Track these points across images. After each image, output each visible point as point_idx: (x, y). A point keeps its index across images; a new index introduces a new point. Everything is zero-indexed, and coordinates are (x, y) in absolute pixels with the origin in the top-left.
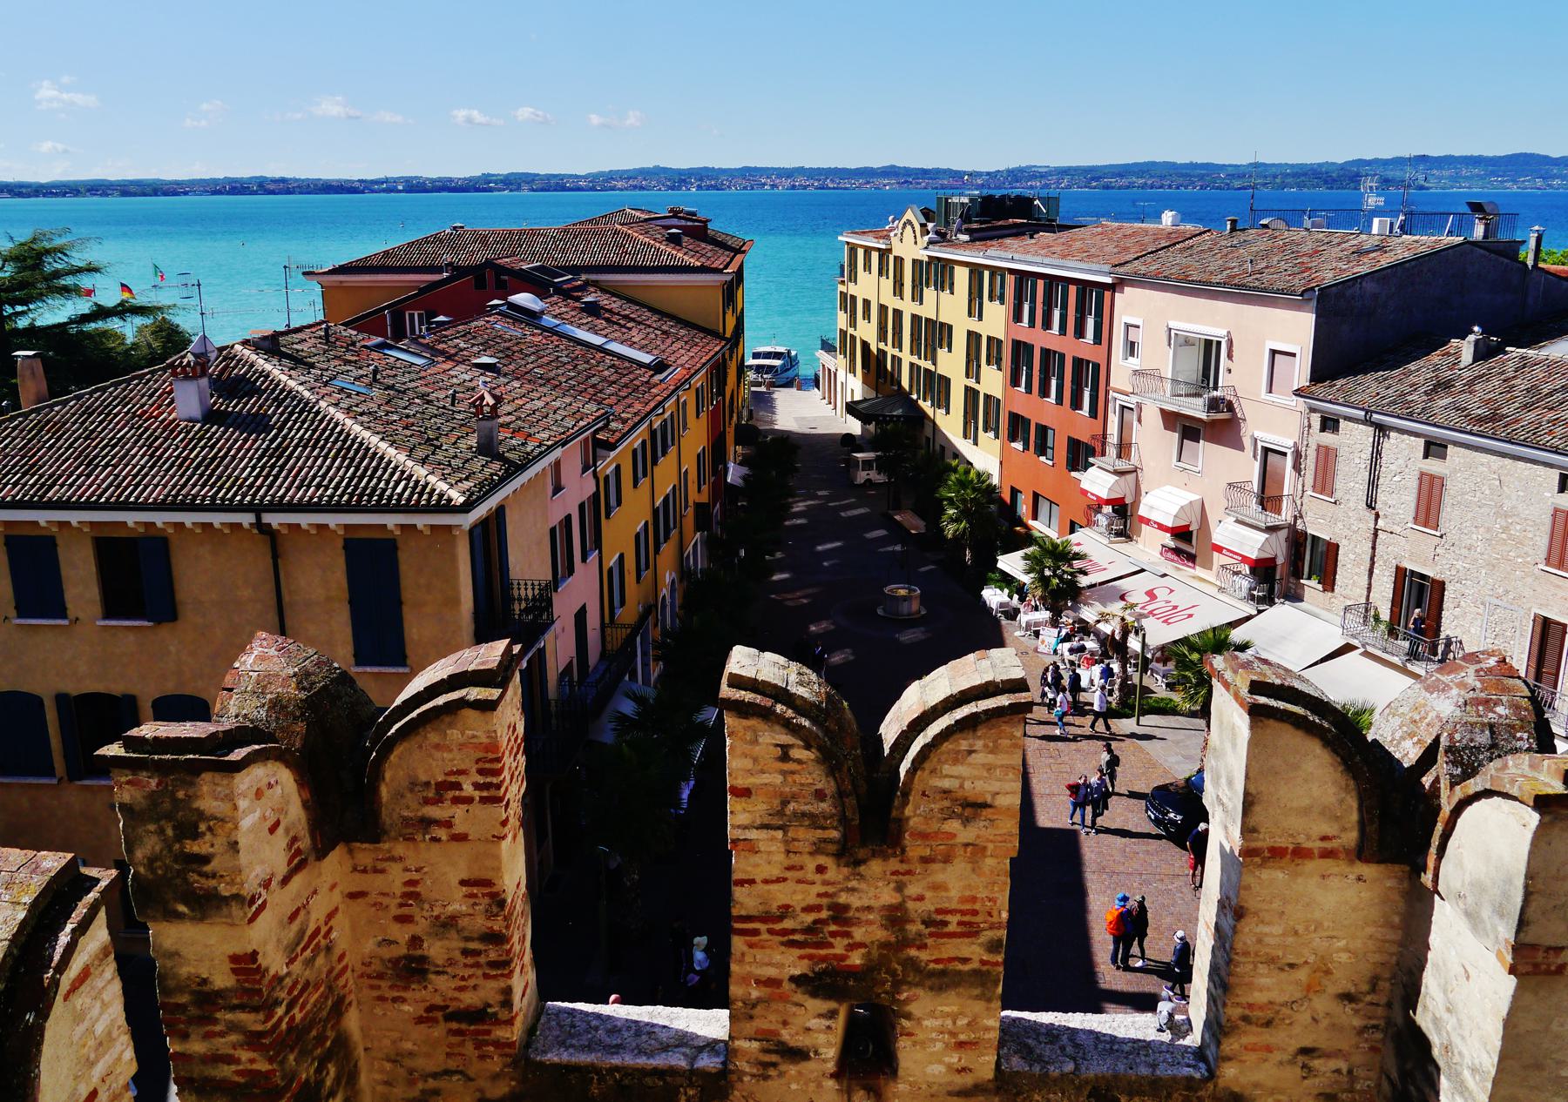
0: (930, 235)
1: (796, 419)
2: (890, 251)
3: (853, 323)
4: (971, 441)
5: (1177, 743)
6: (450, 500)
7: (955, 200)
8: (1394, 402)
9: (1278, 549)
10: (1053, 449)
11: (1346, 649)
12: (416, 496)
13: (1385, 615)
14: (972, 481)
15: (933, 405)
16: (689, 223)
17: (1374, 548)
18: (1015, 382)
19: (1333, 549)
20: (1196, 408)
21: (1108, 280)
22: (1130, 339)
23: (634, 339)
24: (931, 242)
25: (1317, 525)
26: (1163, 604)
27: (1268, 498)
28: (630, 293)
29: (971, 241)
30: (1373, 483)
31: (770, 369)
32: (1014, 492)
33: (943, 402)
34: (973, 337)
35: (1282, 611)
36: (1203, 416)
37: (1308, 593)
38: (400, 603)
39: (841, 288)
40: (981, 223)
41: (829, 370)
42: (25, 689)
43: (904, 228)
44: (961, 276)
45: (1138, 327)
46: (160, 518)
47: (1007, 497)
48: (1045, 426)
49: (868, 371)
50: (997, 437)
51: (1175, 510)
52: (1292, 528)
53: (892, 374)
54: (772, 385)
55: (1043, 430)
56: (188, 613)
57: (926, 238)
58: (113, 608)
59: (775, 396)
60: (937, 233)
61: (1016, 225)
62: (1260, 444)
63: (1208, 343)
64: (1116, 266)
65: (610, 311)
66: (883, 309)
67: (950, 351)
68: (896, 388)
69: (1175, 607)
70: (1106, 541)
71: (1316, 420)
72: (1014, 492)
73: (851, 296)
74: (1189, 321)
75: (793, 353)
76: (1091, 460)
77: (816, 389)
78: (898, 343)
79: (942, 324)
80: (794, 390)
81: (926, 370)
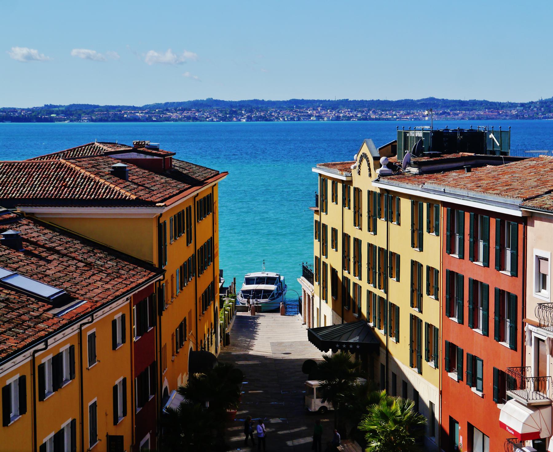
0: (382, 168)
1: (273, 344)
2: (350, 182)
3: (324, 252)
7: (411, 134)
10: (482, 379)
14: (394, 413)
15: (386, 333)
16: (148, 157)
18: (449, 312)
21: (518, 214)
22: (542, 271)
23: (48, 272)
24: (383, 175)
28: (67, 226)
29: (421, 173)
31: (266, 293)
32: (453, 422)
33: (394, 332)
34: (416, 266)
39: (316, 217)
40: (431, 156)
41: (309, 296)
43: (361, 161)
44: (406, 206)
45: (547, 260)
47: (447, 428)
48: (475, 356)
49: (337, 298)
50: (437, 366)
53: (354, 303)
54: (258, 309)
55: (473, 360)
57: (378, 171)
59: (259, 321)
60: (390, 165)
61: (463, 159)
64: (527, 199)
65: (36, 244)
66: (346, 237)
67: (398, 280)
68: (356, 315)
72: (453, 422)
73: (323, 224)
75: (282, 278)
76: (509, 393)
77: (299, 314)
78: (358, 273)
79: (392, 254)
80: (278, 315)
81: (381, 298)
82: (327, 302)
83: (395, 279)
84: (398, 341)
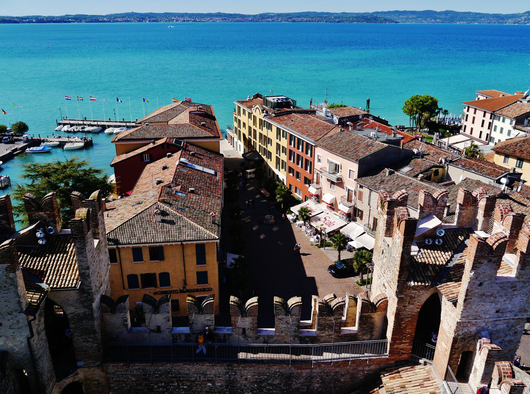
2: (252, 113)
4: (278, 170)
5: (332, 253)
9: (352, 211)
13: (372, 227)
15: (266, 157)
19: (362, 212)
20: (334, 178)
25: (359, 207)
30: (369, 200)
32: (290, 185)
35: (352, 224)
36: (336, 182)
37: (358, 220)
38: (205, 254)
44: (274, 129)
46: (163, 244)
50: (285, 171)
52: (354, 207)
53: (254, 147)
55: (298, 173)
56: (166, 259)
57: (263, 114)
58: (152, 258)
63: (336, 165)
67: (271, 145)
72: (290, 185)
79: (269, 138)
81: (264, 148)
84: (271, 161)
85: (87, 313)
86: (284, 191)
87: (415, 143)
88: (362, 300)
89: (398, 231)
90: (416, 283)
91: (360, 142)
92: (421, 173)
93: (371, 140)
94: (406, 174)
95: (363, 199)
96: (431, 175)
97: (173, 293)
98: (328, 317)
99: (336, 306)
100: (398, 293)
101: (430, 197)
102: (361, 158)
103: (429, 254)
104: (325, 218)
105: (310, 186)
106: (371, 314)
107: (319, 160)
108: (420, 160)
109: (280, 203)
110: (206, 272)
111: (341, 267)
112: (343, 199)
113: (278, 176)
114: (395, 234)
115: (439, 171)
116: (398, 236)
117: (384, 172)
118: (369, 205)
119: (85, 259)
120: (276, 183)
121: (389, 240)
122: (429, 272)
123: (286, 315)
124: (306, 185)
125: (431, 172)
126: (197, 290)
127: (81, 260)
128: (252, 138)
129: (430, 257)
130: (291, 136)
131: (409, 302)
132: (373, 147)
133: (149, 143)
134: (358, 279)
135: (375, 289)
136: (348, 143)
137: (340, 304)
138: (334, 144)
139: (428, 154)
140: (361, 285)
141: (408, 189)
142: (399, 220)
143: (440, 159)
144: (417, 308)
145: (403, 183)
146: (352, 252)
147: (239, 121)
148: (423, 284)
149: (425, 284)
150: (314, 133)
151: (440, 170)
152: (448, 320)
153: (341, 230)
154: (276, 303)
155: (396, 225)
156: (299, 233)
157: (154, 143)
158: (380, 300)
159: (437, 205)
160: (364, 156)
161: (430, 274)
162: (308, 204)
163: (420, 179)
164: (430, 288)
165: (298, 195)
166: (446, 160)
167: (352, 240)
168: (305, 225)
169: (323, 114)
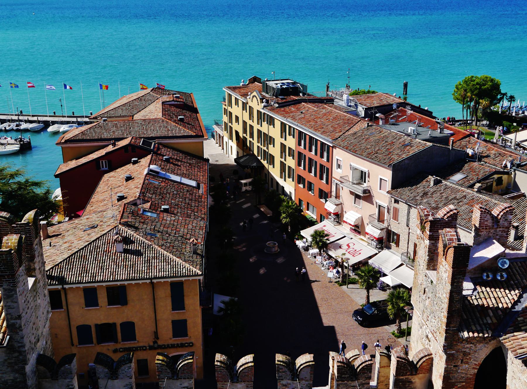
2: (247, 103)
4: (283, 179)
5: (358, 293)
6: (198, 273)
8: (412, 200)
9: (384, 235)
11: (402, 265)
12: (189, 273)
15: (267, 163)
16: (178, 103)
17: (409, 237)
19: (398, 236)
26: (352, 249)
27: (380, 219)
28: (175, 146)
30: (408, 220)
32: (300, 201)
35: (385, 252)
36: (362, 195)
37: (392, 247)
42: (87, 324)
44: (278, 124)
46: (126, 283)
49: (239, 142)
50: (293, 181)
51: (354, 220)
52: (387, 229)
55: (310, 184)
57: (263, 104)
58: (110, 304)
62: (378, 204)
63: (362, 172)
67: (274, 146)
69: (356, 250)
70: (333, 225)
71: (393, 200)
72: (300, 201)
74: (357, 164)
76: (327, 199)
79: (270, 137)
81: (264, 151)
82: (232, 141)
83: (272, 145)
84: (274, 167)
85: (18, 380)
86: (291, 209)
87: (469, 141)
88: (397, 357)
89: (444, 263)
90: (471, 334)
91: (395, 141)
92: (479, 182)
93: (409, 138)
94: (457, 183)
95: (399, 219)
96: (493, 183)
97: (140, 350)
98: (350, 382)
99: (361, 367)
100: (446, 348)
101: (488, 215)
102: (396, 162)
103: (488, 293)
104: (348, 245)
105: (326, 201)
106: (410, 377)
107: (339, 165)
108: (476, 164)
109: (286, 224)
110: (185, 321)
111: (371, 312)
112: (373, 219)
113: (283, 188)
114: (441, 266)
115: (503, 178)
116: (444, 269)
117: (427, 181)
118: (408, 226)
119: (15, 305)
120: (280, 198)
121: (432, 274)
122: (488, 318)
123: (293, 379)
124: (321, 200)
125: (492, 180)
126: (173, 346)
127: (9, 306)
128: (248, 137)
129: (490, 298)
130: (300, 133)
131: (462, 360)
132: (411, 147)
133: (108, 146)
134: (393, 328)
135: (416, 343)
136: (377, 142)
137: (367, 363)
138: (358, 144)
139: (488, 156)
140: (398, 337)
141: (461, 204)
142: (445, 246)
143: (504, 163)
144: (473, 368)
145: (454, 196)
146: (385, 290)
147: (231, 113)
148: (481, 335)
149: (484, 335)
150: (331, 129)
151: (505, 177)
152: (517, 385)
153: (370, 261)
154: (279, 363)
155: (442, 253)
156: (313, 266)
157: (114, 145)
158: (422, 358)
159: (498, 225)
160: (400, 159)
161: (490, 321)
162: (325, 226)
163: (476, 190)
164: (490, 341)
165: (311, 214)
166: (512, 164)
167: (385, 275)
168: (320, 254)
169: (343, 104)
